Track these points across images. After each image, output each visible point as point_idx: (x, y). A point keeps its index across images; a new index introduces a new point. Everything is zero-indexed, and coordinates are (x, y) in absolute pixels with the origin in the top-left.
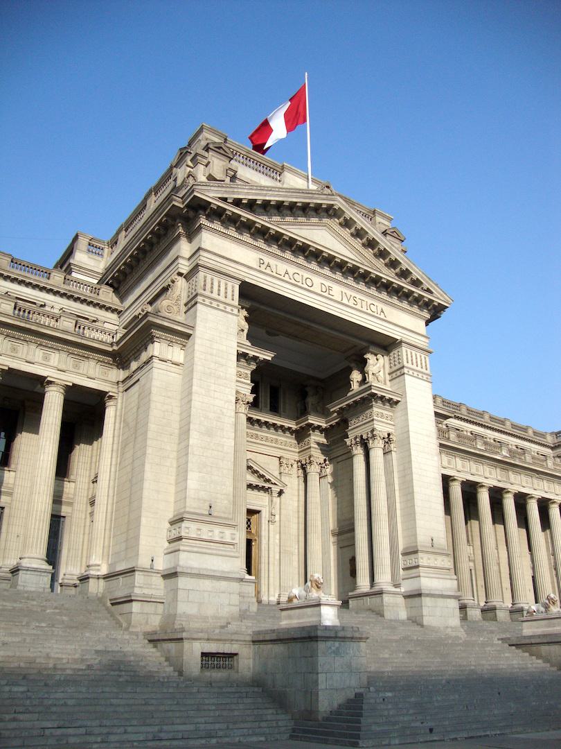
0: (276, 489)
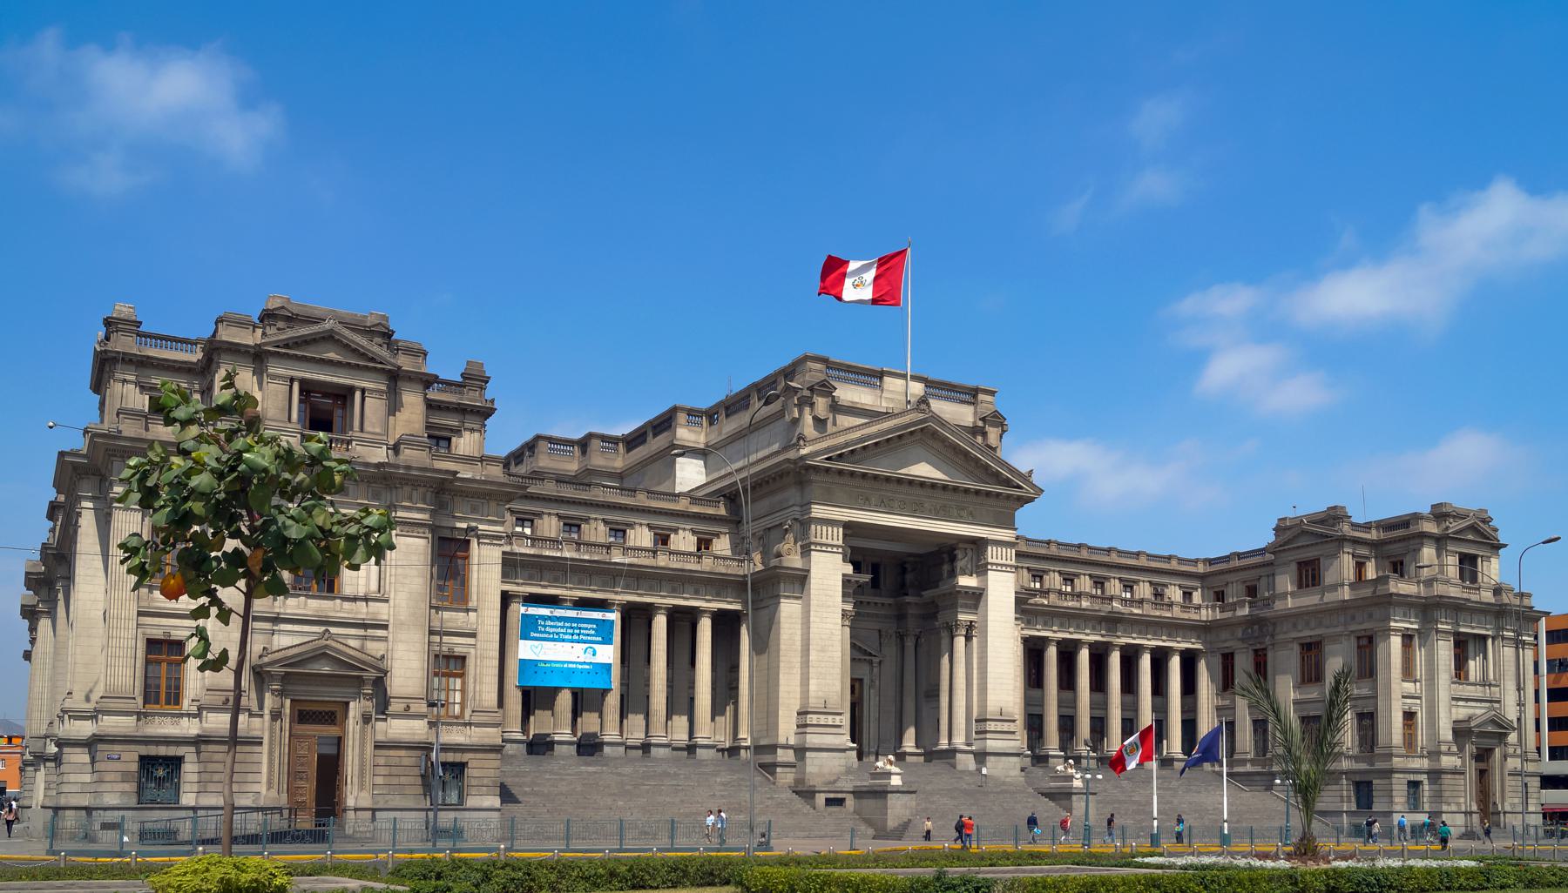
0: (876, 660)
